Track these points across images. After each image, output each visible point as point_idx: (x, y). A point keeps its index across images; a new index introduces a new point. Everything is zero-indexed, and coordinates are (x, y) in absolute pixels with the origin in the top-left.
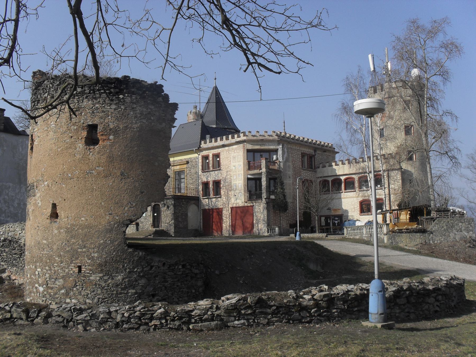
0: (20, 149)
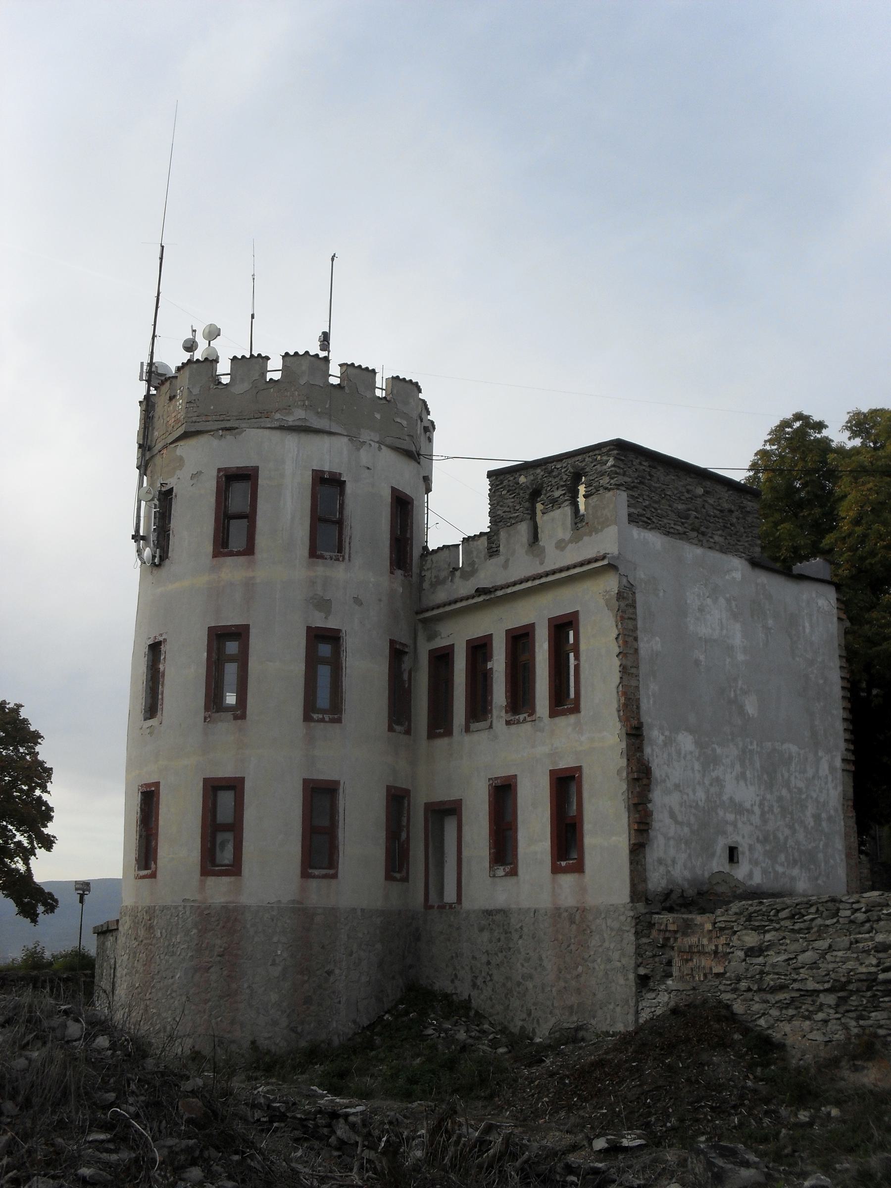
0: (807, 625)
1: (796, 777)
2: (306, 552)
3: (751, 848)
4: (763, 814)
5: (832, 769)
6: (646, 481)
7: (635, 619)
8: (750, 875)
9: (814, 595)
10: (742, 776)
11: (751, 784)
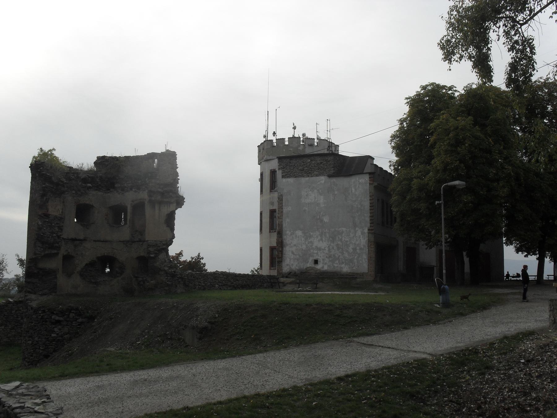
0: (353, 189)
1: (345, 238)
2: (269, 191)
3: (323, 260)
4: (329, 250)
5: (363, 233)
6: (288, 165)
7: (282, 204)
8: (323, 267)
9: (357, 179)
10: (322, 240)
11: (325, 242)
